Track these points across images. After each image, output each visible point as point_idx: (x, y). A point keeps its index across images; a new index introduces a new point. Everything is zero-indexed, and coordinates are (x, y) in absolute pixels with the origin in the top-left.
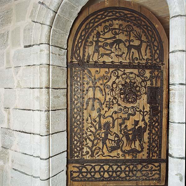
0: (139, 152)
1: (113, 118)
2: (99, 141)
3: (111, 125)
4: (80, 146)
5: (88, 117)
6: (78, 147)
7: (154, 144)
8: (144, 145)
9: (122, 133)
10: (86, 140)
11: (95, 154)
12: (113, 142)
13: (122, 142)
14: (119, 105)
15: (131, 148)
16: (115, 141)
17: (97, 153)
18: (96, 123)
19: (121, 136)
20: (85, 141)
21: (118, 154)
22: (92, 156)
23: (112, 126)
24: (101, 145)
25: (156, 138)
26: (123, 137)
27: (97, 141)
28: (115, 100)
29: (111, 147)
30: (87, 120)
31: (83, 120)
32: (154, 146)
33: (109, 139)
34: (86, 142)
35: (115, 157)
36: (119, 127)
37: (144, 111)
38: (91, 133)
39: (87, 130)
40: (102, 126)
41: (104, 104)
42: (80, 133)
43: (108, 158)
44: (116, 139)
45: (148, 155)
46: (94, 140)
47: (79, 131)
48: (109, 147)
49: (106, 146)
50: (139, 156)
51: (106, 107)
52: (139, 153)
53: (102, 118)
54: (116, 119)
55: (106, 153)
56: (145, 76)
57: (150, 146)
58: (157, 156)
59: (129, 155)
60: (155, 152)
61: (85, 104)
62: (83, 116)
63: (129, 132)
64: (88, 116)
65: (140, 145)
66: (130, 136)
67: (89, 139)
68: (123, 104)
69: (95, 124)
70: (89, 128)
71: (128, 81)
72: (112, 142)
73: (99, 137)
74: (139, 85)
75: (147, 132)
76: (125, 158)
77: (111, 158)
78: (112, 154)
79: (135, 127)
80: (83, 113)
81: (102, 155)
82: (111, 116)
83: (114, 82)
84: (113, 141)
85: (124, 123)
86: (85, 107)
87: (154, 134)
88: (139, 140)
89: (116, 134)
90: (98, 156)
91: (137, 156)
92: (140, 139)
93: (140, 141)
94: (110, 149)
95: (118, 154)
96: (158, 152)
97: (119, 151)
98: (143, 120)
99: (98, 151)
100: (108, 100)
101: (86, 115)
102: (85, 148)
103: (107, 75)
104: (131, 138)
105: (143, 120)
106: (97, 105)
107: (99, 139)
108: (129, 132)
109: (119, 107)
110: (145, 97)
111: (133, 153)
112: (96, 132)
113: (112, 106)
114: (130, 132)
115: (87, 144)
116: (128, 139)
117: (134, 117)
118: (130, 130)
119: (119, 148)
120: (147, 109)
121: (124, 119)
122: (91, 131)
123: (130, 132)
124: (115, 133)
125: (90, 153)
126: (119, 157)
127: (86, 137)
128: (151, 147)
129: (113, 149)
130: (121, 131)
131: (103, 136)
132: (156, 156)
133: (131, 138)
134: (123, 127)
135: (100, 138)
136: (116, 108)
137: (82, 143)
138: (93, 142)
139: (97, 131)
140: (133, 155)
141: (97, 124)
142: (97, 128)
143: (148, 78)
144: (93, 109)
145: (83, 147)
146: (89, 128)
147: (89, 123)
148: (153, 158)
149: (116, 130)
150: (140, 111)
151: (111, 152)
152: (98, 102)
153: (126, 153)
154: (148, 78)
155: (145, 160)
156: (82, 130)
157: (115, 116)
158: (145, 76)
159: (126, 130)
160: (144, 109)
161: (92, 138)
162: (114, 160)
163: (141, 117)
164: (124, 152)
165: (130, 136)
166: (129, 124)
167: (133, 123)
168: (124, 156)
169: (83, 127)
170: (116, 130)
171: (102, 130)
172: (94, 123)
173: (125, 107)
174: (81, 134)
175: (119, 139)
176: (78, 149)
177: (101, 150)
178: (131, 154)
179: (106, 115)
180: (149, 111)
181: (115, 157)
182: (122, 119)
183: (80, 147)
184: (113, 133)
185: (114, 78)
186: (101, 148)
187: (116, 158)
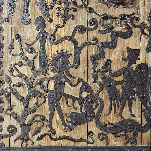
1: (75, 43)
2: (41, 100)
3: (71, 60)
5: (13, 41)
9: (99, 79)
13: (99, 103)
15: (122, 117)
16: (81, 100)
17: (38, 131)
18: (34, 55)
19: (95, 87)
20: (6, 101)
21: (90, 134)
22: (24, 138)
23: (75, 62)
24: (45, 110)
26: (101, 90)
33: (67, 96)
34: (9, 101)
35: (81, 140)
36: (91, 65)
39: (12, 71)
40: (49, 62)
41: (52, 8)
44: (84, 95)
46: (30, 97)
48: (67, 116)
49: (60, 112)
51: (58, 16)
53: (48, 42)
55: (60, 132)
59: (116, 137)
64: (13, 37)
65: (142, 110)
66: (120, 88)
67: (16, 93)
69: (31, 56)
70: (17, 67)
76: (107, 143)
77: (72, 144)
78: (74, 134)
79: (130, 65)
81: (49, 135)
82: (71, 39)
84: (77, 99)
85: (101, 55)
88: (140, 98)
89: (84, 83)
90: (40, 138)
91: (138, 138)
92: (143, 97)
94: (69, 120)
95: (90, 134)
97: (92, 126)
99: (40, 124)
102: (6, 118)
104: (120, 92)
107: (41, 95)
108: (116, 79)
109: (91, 16)
112: (34, 77)
113: (74, 14)
115: (11, 109)
116: (113, 96)
117: (127, 41)
118: (118, 74)
119: (91, 117)
121: (102, 46)
123: (116, 79)
124: (80, 80)
125: (19, 131)
126: (93, 142)
127: (9, 91)
130: (95, 76)
131: (52, 86)
133: (120, 92)
134: (101, 64)
135: (42, 91)
139: (36, 74)
140: (127, 137)
141: (35, 57)
142: (37, 68)
144: (25, 20)
147: (15, 56)
151: (70, 129)
157: (80, 38)
161: (24, 92)
164: (103, 127)
165: (120, 88)
166: (116, 57)
167: (126, 56)
168: (105, 138)
171: (49, 72)
172: (28, 54)
175: (91, 95)
177: (46, 123)
178: (123, 133)
179: (59, 35)
181: (81, 140)
182: (99, 47)
184: (76, 81)
186: (47, 118)
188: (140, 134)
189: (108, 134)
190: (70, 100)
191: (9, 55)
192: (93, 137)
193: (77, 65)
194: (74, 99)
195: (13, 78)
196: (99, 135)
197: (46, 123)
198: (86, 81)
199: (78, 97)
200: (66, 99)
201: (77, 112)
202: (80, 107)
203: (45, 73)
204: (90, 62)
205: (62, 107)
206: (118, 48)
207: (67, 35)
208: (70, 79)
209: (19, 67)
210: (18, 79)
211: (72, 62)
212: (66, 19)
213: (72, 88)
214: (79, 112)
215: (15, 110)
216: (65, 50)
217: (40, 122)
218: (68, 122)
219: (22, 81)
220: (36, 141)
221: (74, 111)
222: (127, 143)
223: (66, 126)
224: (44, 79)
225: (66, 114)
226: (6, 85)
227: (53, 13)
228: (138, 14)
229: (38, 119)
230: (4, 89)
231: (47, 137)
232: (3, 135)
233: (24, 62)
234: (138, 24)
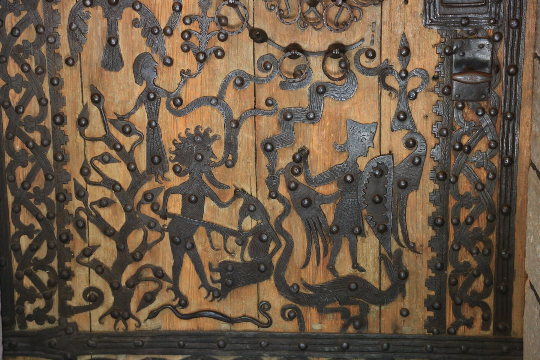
0: (383, 298)
1: (227, 110)
2: (153, 236)
3: (218, 150)
4: (54, 264)
5: (86, 107)
6: (43, 265)
7: (465, 256)
8: (408, 258)
9: (283, 190)
10: (82, 229)
11: (133, 306)
12: (232, 242)
13: (283, 243)
14: (259, 36)
16: (240, 236)
17: (148, 299)
18: (135, 138)
19: (275, 208)
20: (77, 236)
22: (120, 312)
24: (164, 256)
25: (482, 222)
27: (145, 237)
28: (232, 10)
29: (223, 267)
30: (83, 122)
31: (63, 122)
32: (467, 264)
33: (211, 227)
34: (84, 237)
36: (264, 160)
38: (108, 193)
40: (168, 155)
42: (47, 191)
43: (207, 324)
44: (249, 224)
45: (431, 314)
46: (127, 229)
47: (39, 182)
50: (382, 320)
51: (187, 51)
52: (381, 303)
54: (243, 118)
55: (197, 300)
57: (443, 267)
58: (486, 321)
59: (322, 311)
60: (477, 301)
61: (63, 32)
62: (58, 99)
63: (322, 190)
64: (87, 99)
65: (382, 257)
66: (329, 211)
68: (282, 35)
70: (100, 165)
72: (225, 240)
73: (153, 215)
75: (428, 186)
76: (302, 326)
77: (224, 326)
78: (230, 306)
80: (56, 84)
81: (174, 309)
82: (218, 101)
86: (64, 51)
87: (464, 201)
90: (153, 315)
93: (383, 233)
94: (217, 276)
95: (264, 307)
96: (490, 301)
97: (269, 291)
98: (403, 117)
99: (153, 286)
100: (197, 10)
101: (74, 98)
105: (403, 117)
106: (132, 42)
107: (152, 225)
108: (322, 190)
109: (263, 49)
111: (344, 301)
112: (134, 188)
113: (222, 45)
114: (329, 189)
115: (88, 252)
116: (313, 227)
117: (346, 105)
120: (427, 56)
122: (109, 183)
124: (238, 193)
125: (110, 299)
126: (270, 323)
127: (83, 215)
128: (450, 270)
129: (231, 279)
130: (272, 183)
131: (175, 205)
132: (478, 323)
135: (157, 217)
136: (243, 55)
137: (60, 246)
138: (120, 238)
140: (346, 315)
142: (142, 164)
144: (112, 61)
145: (67, 264)
146: (100, 165)
147: (94, 140)
148: (462, 331)
149: (246, 175)
150: (383, 72)
151: (220, 295)
152: (135, 23)
153: (308, 301)
155: (417, 342)
156: (56, 176)
157: (237, 102)
159: (301, 179)
160: (405, 52)
161: (116, 218)
162: (241, 337)
163: (390, 106)
169: (62, 158)
170: (246, 175)
173: (294, 50)
174: (52, 196)
176: (44, 276)
177: (166, 284)
179: (189, 94)
181: (245, 319)
183: (52, 269)
184: (230, 194)
186: (169, 272)
187: (251, 326)
188: (374, 308)
189: (303, 309)
190: (218, 238)
191: (80, 140)
192: (270, 312)
193: (230, 162)
194: (226, 233)
195: (91, 189)
196: (283, 310)
197: (166, 284)
198: (254, 194)
199: (235, 228)
200: (209, 236)
201: (234, 260)
202: (240, 249)
203: (160, 178)
204: (261, 153)
205: (199, 248)
206: (326, 122)
207: (206, 93)
208: (216, 190)
209: (103, 166)
210: (101, 190)
211: (222, 153)
212: (202, 58)
213: (222, 210)
214: (239, 260)
215: (99, 255)
216: (205, 127)
217: (155, 281)
218: (214, 282)
219: (112, 196)
220: (145, 320)
221: (228, 258)
222: (345, 327)
223: (210, 290)
224: (160, 189)
225: (210, 265)
226: (75, 204)
227: (172, 45)
228: (372, 42)
229: (150, 274)
230: (73, 210)
231: (167, 312)
232: (74, 308)
233: (113, 153)
234: (373, 64)
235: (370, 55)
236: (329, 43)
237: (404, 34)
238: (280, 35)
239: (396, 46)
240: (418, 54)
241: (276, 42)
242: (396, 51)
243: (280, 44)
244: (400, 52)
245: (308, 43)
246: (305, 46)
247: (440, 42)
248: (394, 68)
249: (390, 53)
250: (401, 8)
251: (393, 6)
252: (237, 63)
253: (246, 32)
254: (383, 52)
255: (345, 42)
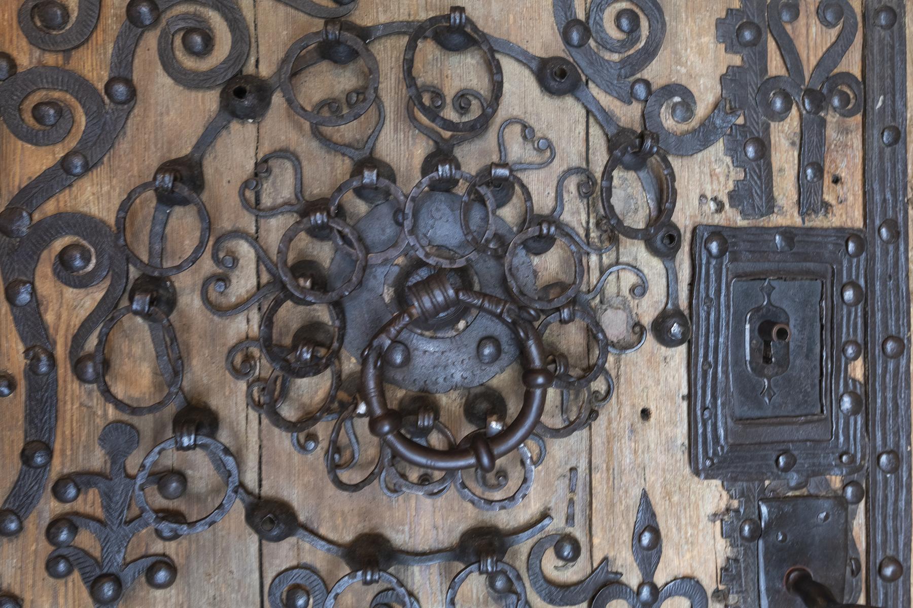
14: (272, 517)
37: (660, 579)
56: (656, 72)
71: (403, 150)
74: (576, 215)
83: (183, 179)
103: (51, 59)
110: (657, 378)
143: (702, 109)
154: (702, 109)
158: (656, 72)
180: (728, 572)
185: (173, 113)
235: (567, 551)
236: (462, 527)
237: (645, 495)
238: (333, 514)
239: (628, 524)
240: (676, 539)
241: (323, 531)
242: (626, 536)
243: (332, 536)
244: (637, 537)
245: (407, 528)
246: (399, 538)
247: (728, 510)
248: (624, 579)
249: (612, 543)
250: (633, 431)
251: (614, 425)
252: (212, 593)
253: (237, 510)
254: (596, 541)
255: (505, 519)
